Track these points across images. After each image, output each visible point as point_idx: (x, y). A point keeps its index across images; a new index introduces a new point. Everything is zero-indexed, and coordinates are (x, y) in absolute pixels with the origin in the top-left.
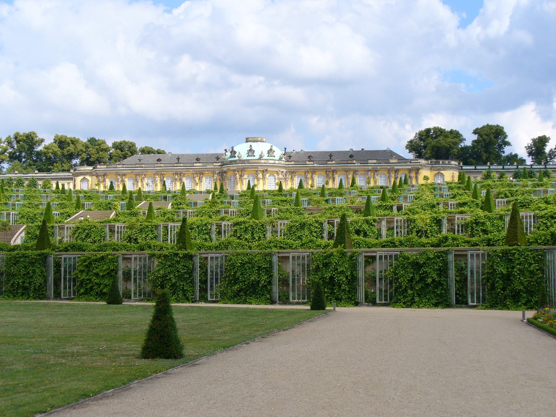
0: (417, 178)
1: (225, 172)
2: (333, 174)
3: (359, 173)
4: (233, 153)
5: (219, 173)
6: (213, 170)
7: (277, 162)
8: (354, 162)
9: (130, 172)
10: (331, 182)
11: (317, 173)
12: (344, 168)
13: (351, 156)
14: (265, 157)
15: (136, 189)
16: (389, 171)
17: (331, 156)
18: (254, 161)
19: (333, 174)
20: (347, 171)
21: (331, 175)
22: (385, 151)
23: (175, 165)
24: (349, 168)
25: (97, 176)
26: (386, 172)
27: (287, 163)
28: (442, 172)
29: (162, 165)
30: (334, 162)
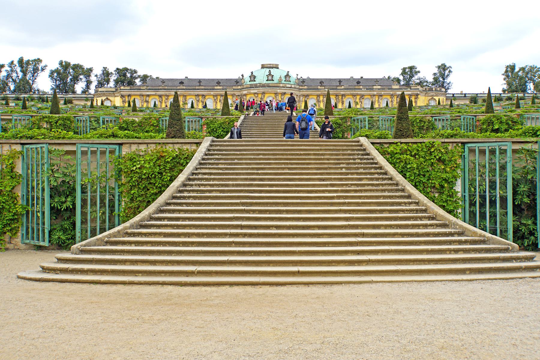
1: (245, 95)
2: (342, 98)
3: (366, 97)
4: (253, 77)
5: (239, 96)
6: (232, 93)
7: (293, 86)
8: (361, 87)
12: (352, 92)
13: (358, 82)
14: (283, 82)
19: (342, 98)
20: (354, 96)
22: (381, 79)
25: (122, 96)
28: (435, 97)
30: (343, 87)
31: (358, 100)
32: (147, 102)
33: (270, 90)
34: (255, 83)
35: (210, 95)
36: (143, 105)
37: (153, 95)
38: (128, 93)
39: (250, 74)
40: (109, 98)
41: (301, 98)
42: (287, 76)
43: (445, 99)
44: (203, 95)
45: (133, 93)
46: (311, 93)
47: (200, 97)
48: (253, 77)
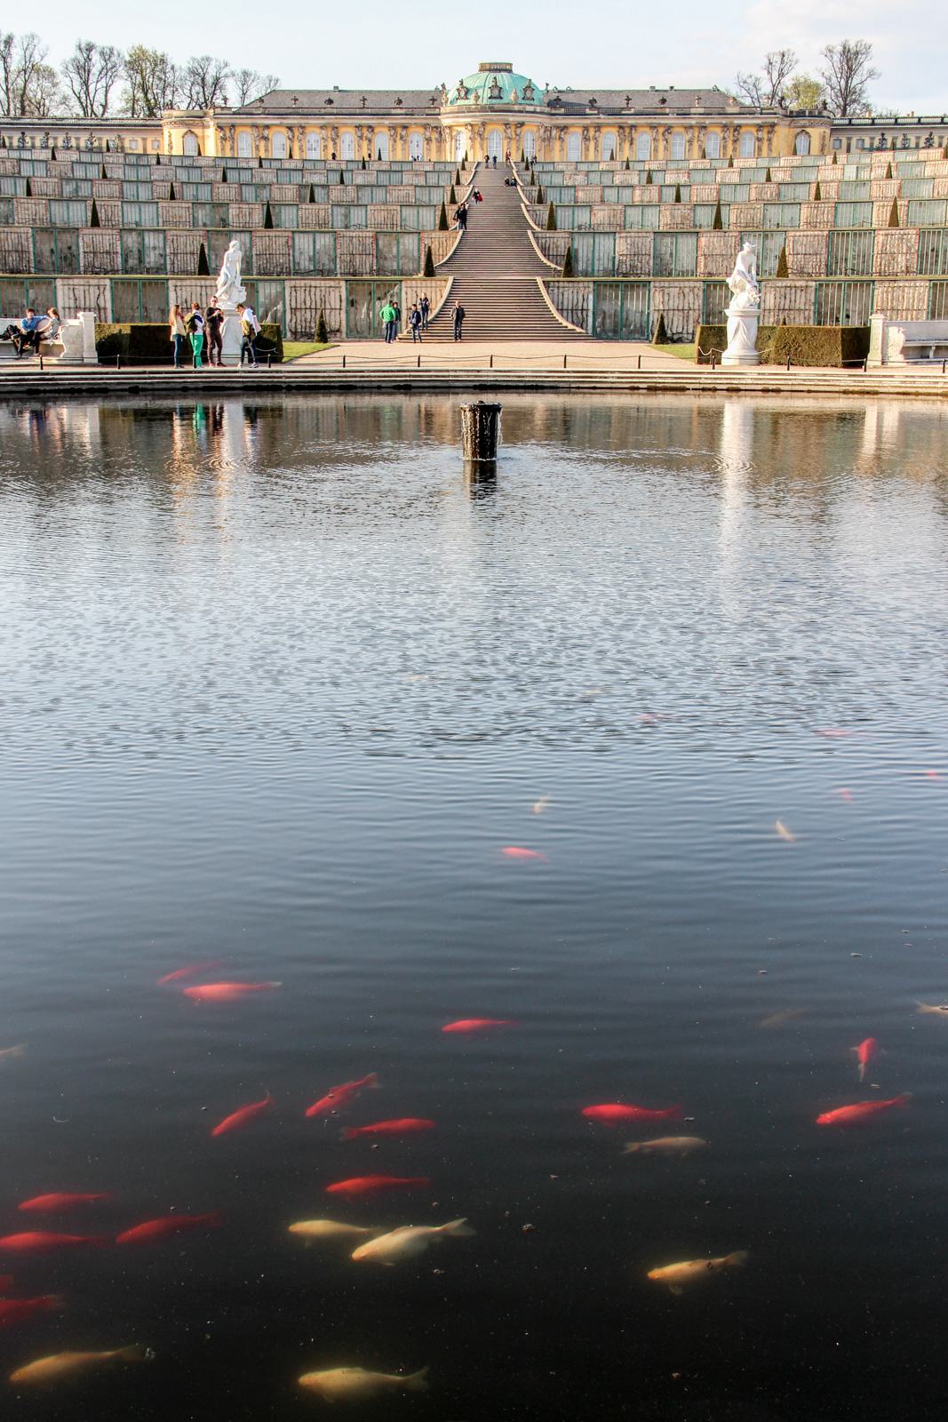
0: (769, 140)
3: (675, 130)
6: (424, 122)
7: (538, 109)
9: (278, 122)
10: (627, 145)
11: (604, 130)
12: (649, 121)
19: (630, 133)
20: (653, 127)
24: (658, 121)
25: (220, 128)
26: (718, 130)
28: (808, 130)
31: (661, 137)
33: (495, 118)
35: (382, 125)
36: (257, 148)
37: (277, 125)
40: (193, 130)
41: (554, 132)
42: (529, 87)
43: (828, 131)
45: (238, 121)
46: (572, 121)
47: (365, 130)
48: (465, 91)
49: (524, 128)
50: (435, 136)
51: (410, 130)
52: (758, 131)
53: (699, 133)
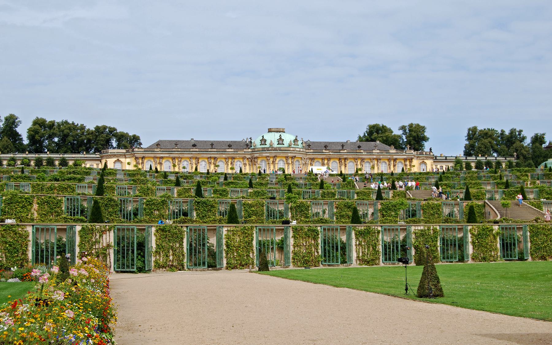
1: (257, 158)
2: (345, 161)
5: (250, 158)
6: (243, 156)
7: (301, 150)
8: (362, 151)
11: (332, 161)
15: (251, 172)
16: (389, 160)
17: (343, 146)
18: (285, 149)
19: (345, 161)
20: (355, 159)
21: (343, 162)
23: (209, 150)
25: (136, 158)
27: (307, 151)
28: (425, 161)
29: (197, 150)
30: (345, 151)
31: (359, 163)
32: (161, 164)
34: (266, 146)
37: (167, 157)
38: (143, 155)
39: (261, 138)
44: (215, 158)
47: (213, 161)
49: (296, 159)
50: (247, 162)
51: (236, 160)
52: (404, 161)
53: (378, 162)
